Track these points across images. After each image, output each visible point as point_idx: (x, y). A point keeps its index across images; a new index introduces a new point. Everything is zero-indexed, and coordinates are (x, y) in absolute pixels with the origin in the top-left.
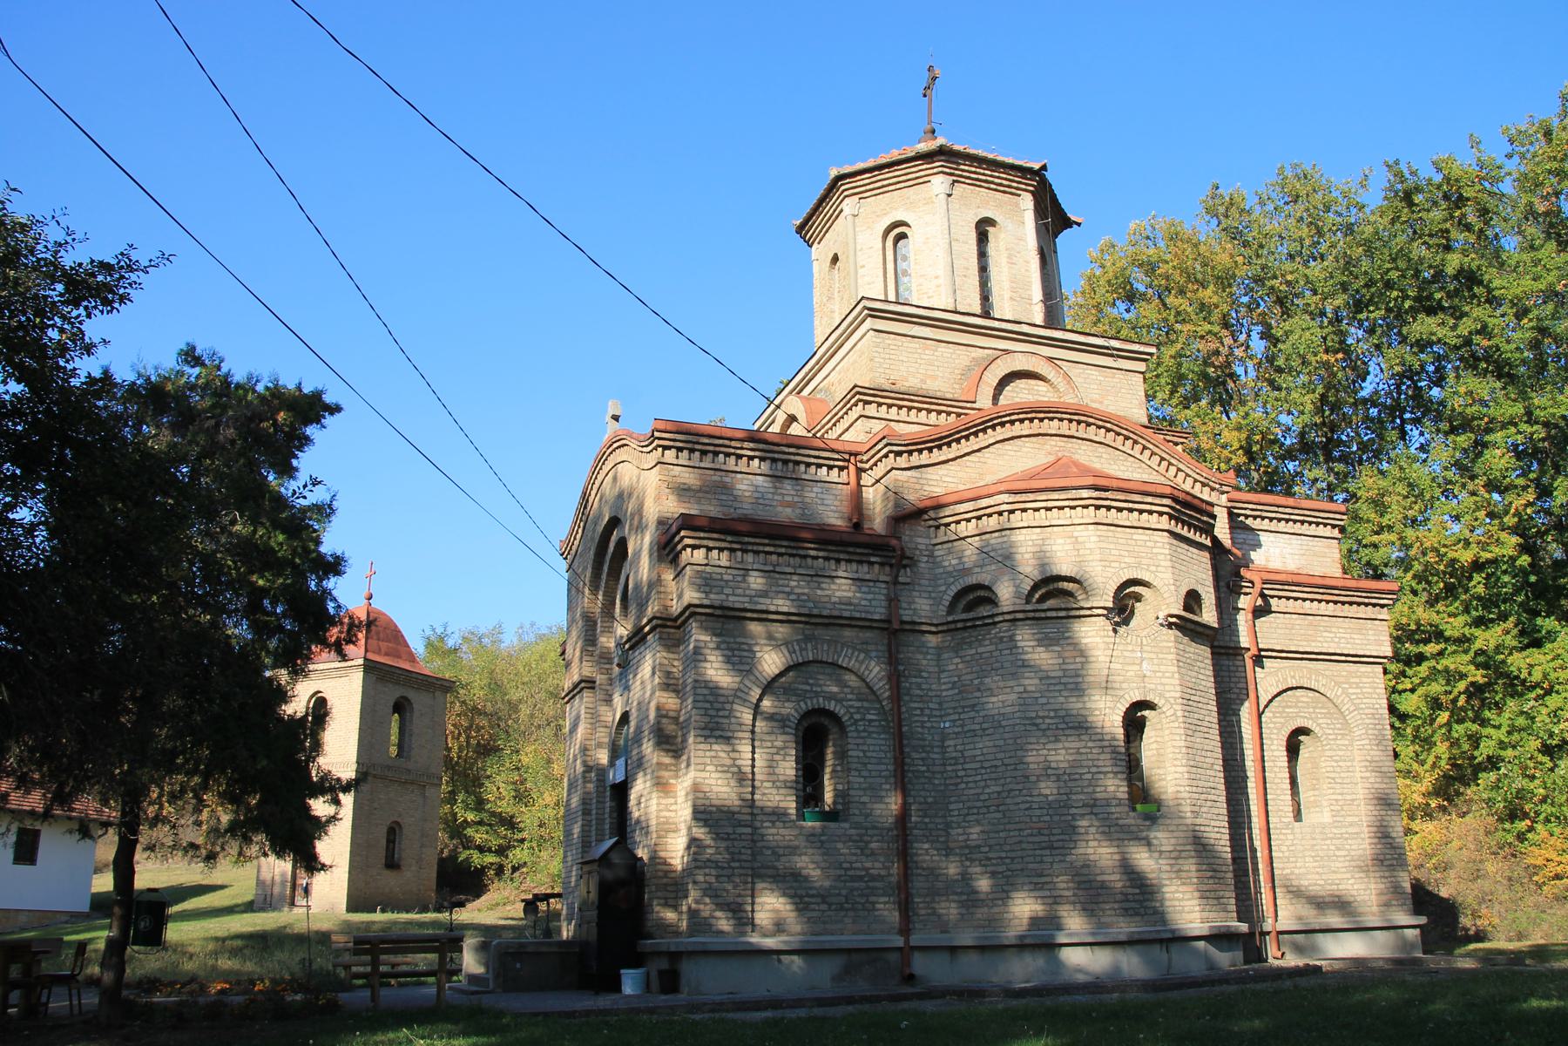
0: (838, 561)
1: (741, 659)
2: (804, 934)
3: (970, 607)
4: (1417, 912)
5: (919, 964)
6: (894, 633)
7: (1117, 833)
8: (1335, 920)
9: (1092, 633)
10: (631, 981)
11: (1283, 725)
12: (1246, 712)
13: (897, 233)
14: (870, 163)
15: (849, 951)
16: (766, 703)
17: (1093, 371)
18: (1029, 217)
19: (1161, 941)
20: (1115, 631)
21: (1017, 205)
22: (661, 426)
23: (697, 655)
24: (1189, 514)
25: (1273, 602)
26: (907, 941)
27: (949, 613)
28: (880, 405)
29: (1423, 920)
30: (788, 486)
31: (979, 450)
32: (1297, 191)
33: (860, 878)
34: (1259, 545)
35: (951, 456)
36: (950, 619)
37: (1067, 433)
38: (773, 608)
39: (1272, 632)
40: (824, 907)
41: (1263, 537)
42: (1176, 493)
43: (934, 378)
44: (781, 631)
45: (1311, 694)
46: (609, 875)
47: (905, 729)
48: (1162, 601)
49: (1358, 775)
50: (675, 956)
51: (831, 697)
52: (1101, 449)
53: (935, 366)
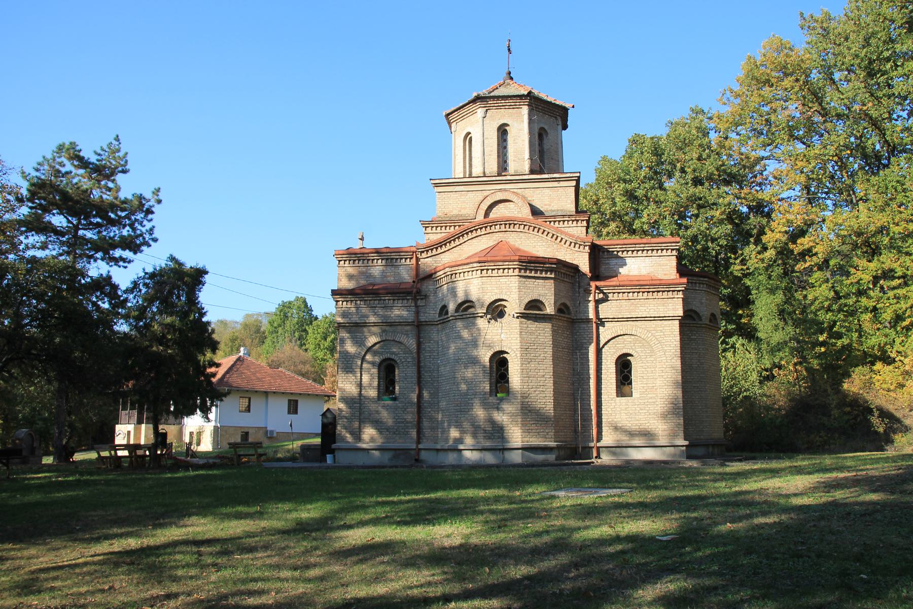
5: (424, 455)
6: (419, 326)
7: (486, 406)
8: (637, 442)
9: (482, 323)
10: (329, 457)
12: (592, 349)
13: (468, 137)
14: (453, 109)
15: (395, 450)
16: (369, 357)
17: (547, 190)
19: (500, 450)
29: (686, 443)
34: (625, 264)
39: (605, 310)
41: (628, 260)
43: (465, 208)
46: (325, 421)
48: (514, 306)
51: (393, 353)
52: (521, 234)
53: (464, 204)
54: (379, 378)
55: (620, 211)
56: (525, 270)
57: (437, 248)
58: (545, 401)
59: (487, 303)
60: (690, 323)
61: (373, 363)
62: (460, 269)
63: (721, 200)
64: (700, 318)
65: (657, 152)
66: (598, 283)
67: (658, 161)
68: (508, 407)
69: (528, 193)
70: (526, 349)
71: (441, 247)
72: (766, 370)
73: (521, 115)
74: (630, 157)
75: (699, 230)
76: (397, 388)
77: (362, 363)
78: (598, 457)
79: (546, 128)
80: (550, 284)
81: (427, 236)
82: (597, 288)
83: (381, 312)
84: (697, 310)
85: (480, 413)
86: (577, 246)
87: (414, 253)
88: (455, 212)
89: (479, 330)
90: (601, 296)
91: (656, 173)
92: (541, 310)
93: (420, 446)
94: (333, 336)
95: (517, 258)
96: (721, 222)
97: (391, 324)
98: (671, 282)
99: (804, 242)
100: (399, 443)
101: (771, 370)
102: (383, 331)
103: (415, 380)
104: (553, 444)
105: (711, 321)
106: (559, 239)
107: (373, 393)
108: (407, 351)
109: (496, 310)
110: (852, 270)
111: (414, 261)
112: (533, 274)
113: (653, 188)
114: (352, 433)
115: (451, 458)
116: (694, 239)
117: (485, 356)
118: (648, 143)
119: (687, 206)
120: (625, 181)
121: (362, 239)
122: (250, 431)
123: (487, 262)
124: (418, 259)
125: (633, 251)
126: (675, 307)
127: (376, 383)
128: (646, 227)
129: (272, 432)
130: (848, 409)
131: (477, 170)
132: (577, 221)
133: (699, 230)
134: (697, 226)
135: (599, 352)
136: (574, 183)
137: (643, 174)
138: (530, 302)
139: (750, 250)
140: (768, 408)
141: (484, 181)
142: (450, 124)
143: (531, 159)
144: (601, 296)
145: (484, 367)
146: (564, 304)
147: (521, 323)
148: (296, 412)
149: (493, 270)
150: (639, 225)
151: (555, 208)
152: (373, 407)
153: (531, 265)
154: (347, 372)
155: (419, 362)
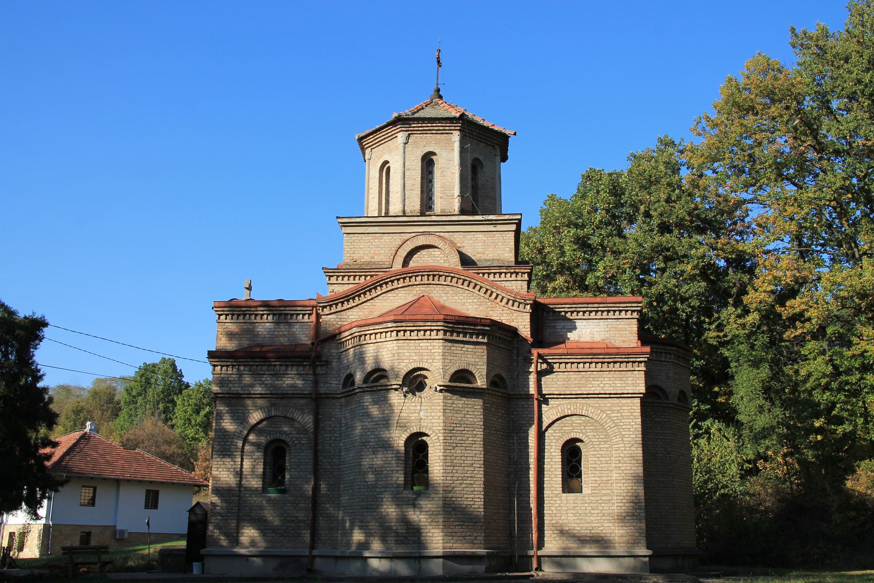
0: (287, 366)
1: (240, 417)
2: (266, 548)
4: (648, 548)
5: (319, 564)
6: (317, 400)
7: (399, 502)
9: (396, 398)
10: (196, 568)
11: (560, 437)
13: (385, 168)
15: (282, 556)
16: (252, 437)
17: (480, 235)
18: (457, 145)
19: (415, 558)
20: (405, 396)
21: (450, 139)
22: (217, 305)
25: (556, 366)
26: (311, 552)
27: (343, 388)
28: (338, 276)
29: (649, 552)
30: (282, 326)
31: (372, 299)
33: (293, 521)
34: (575, 328)
35: (354, 305)
36: (345, 390)
37: (427, 282)
38: (253, 392)
39: (550, 384)
40: (274, 535)
41: (578, 323)
42: (449, 318)
44: (259, 402)
45: (583, 418)
46: (193, 518)
47: (320, 447)
48: (436, 378)
49: (613, 465)
51: (285, 433)
52: (448, 288)
53: (378, 249)
54: (265, 464)
55: (570, 261)
56: (452, 333)
57: (342, 303)
58: (473, 496)
59: (403, 372)
60: (653, 402)
61: (257, 445)
62: (371, 330)
63: (693, 252)
64: (666, 396)
65: (616, 191)
66: (542, 351)
67: (617, 201)
68: (426, 504)
69: (458, 239)
70: (450, 431)
71: (348, 301)
72: (749, 462)
73: (451, 143)
74: (584, 196)
75: (665, 287)
76: (287, 476)
77: (244, 445)
78: (539, 568)
79: (481, 158)
80: (482, 351)
81: (331, 287)
82: (540, 356)
83: (268, 379)
84: (663, 386)
85: (390, 510)
86: (516, 304)
87: (315, 307)
88: (367, 259)
89: (391, 406)
90: (544, 366)
91: (614, 217)
92: (471, 383)
93: (315, 552)
94: (207, 409)
95: (442, 317)
96: (693, 278)
98: (630, 351)
99: (795, 305)
100: (287, 549)
101: (755, 462)
102: (272, 405)
103: (310, 467)
104: (482, 551)
105: (679, 400)
106: (494, 295)
107: (255, 483)
108: (303, 430)
109: (414, 382)
110: (855, 340)
111: (313, 318)
112: (461, 338)
113: (610, 235)
114: (227, 535)
115: (354, 568)
116: (660, 298)
117: (399, 439)
118: (605, 179)
119: (652, 258)
120: (576, 226)
121: (249, 288)
122: (94, 531)
123: (404, 322)
124: (318, 316)
125: (584, 312)
126: (636, 382)
127: (260, 469)
128: (601, 283)
129: (122, 532)
130: (853, 514)
131: (395, 208)
132: (517, 273)
133: (665, 287)
134: (662, 282)
136: (514, 227)
137: (599, 218)
138: (456, 372)
139: (729, 313)
140: (752, 510)
141: (404, 221)
142: (363, 150)
143: (462, 195)
144: (544, 366)
145: (398, 452)
146: (499, 376)
147: (445, 398)
148: (155, 506)
149: (411, 331)
150: (593, 280)
151: (490, 257)
152: (256, 500)
153: (459, 327)
154: (224, 456)
155: (316, 444)
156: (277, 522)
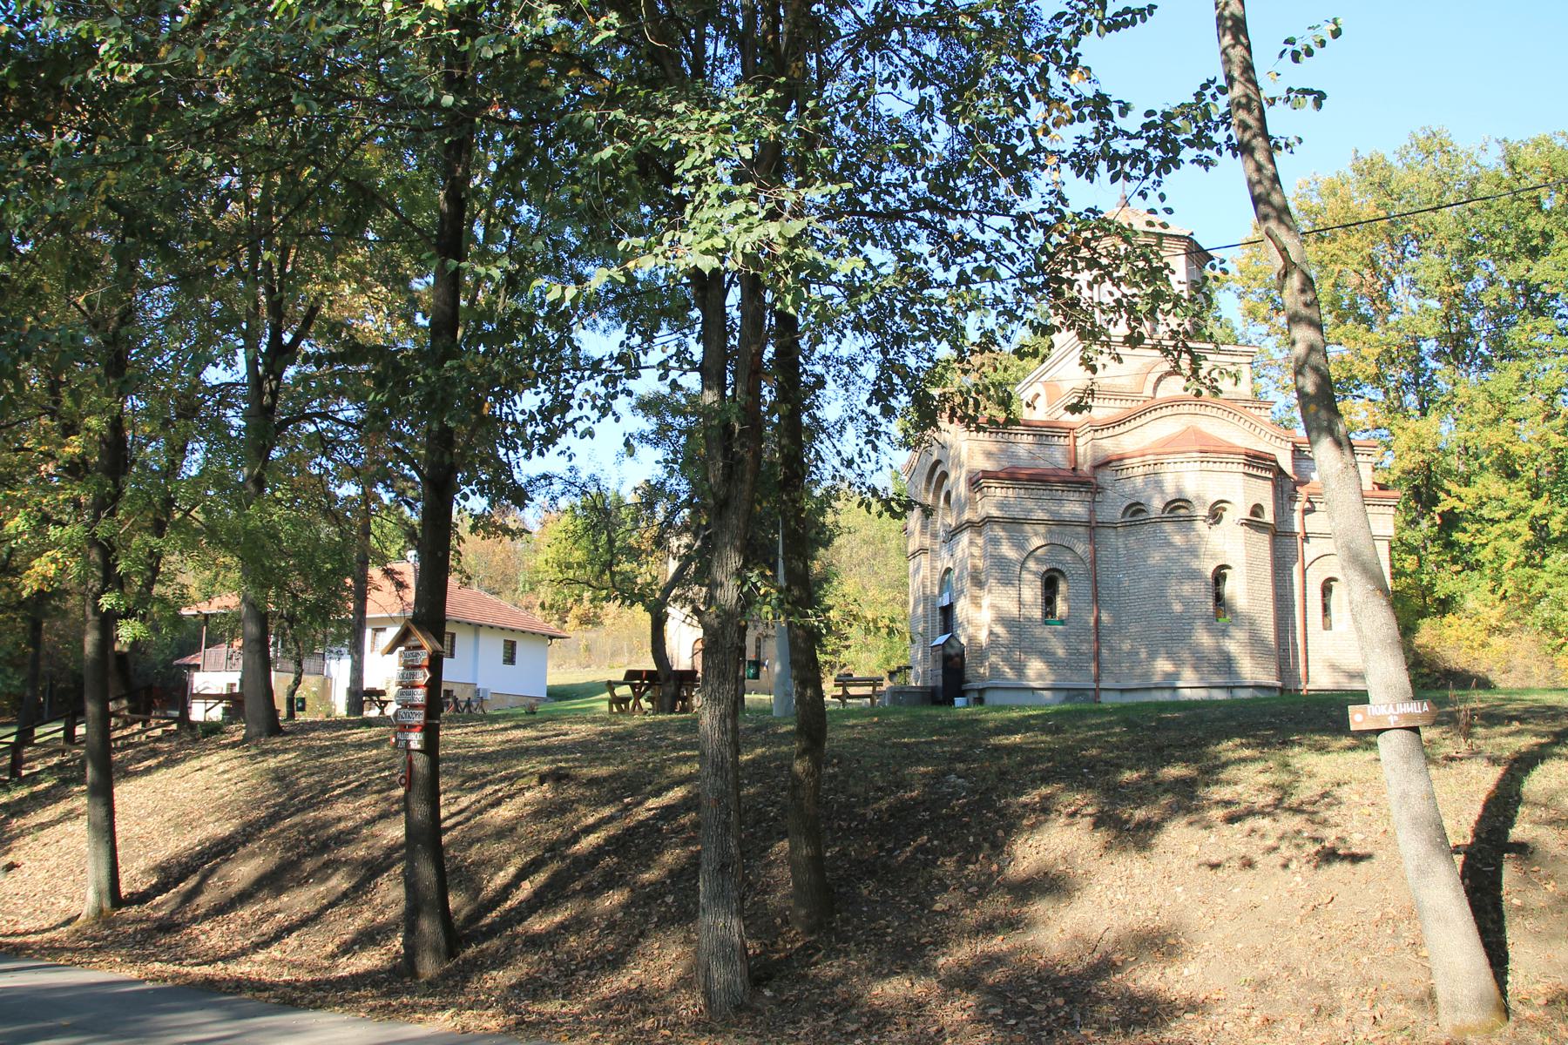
3: (1133, 515)
6: (1093, 527)
7: (1210, 629)
9: (1201, 526)
10: (959, 701)
12: (1296, 570)
16: (1031, 565)
23: (995, 541)
24: (1257, 461)
32: (1433, 145)
39: (1314, 523)
48: (1238, 511)
50: (982, 691)
51: (1060, 562)
61: (1035, 573)
80: (1268, 486)
85: (1204, 639)
97: (1061, 523)
100: (1078, 681)
102: (1049, 532)
104: (1279, 684)
107: (1037, 613)
110: (1442, 495)
117: (1209, 569)
123: (1211, 452)
129: (485, 691)
135: (1304, 571)
144: (1307, 505)
152: (1038, 631)
153: (1257, 461)
156: (1061, 652)
